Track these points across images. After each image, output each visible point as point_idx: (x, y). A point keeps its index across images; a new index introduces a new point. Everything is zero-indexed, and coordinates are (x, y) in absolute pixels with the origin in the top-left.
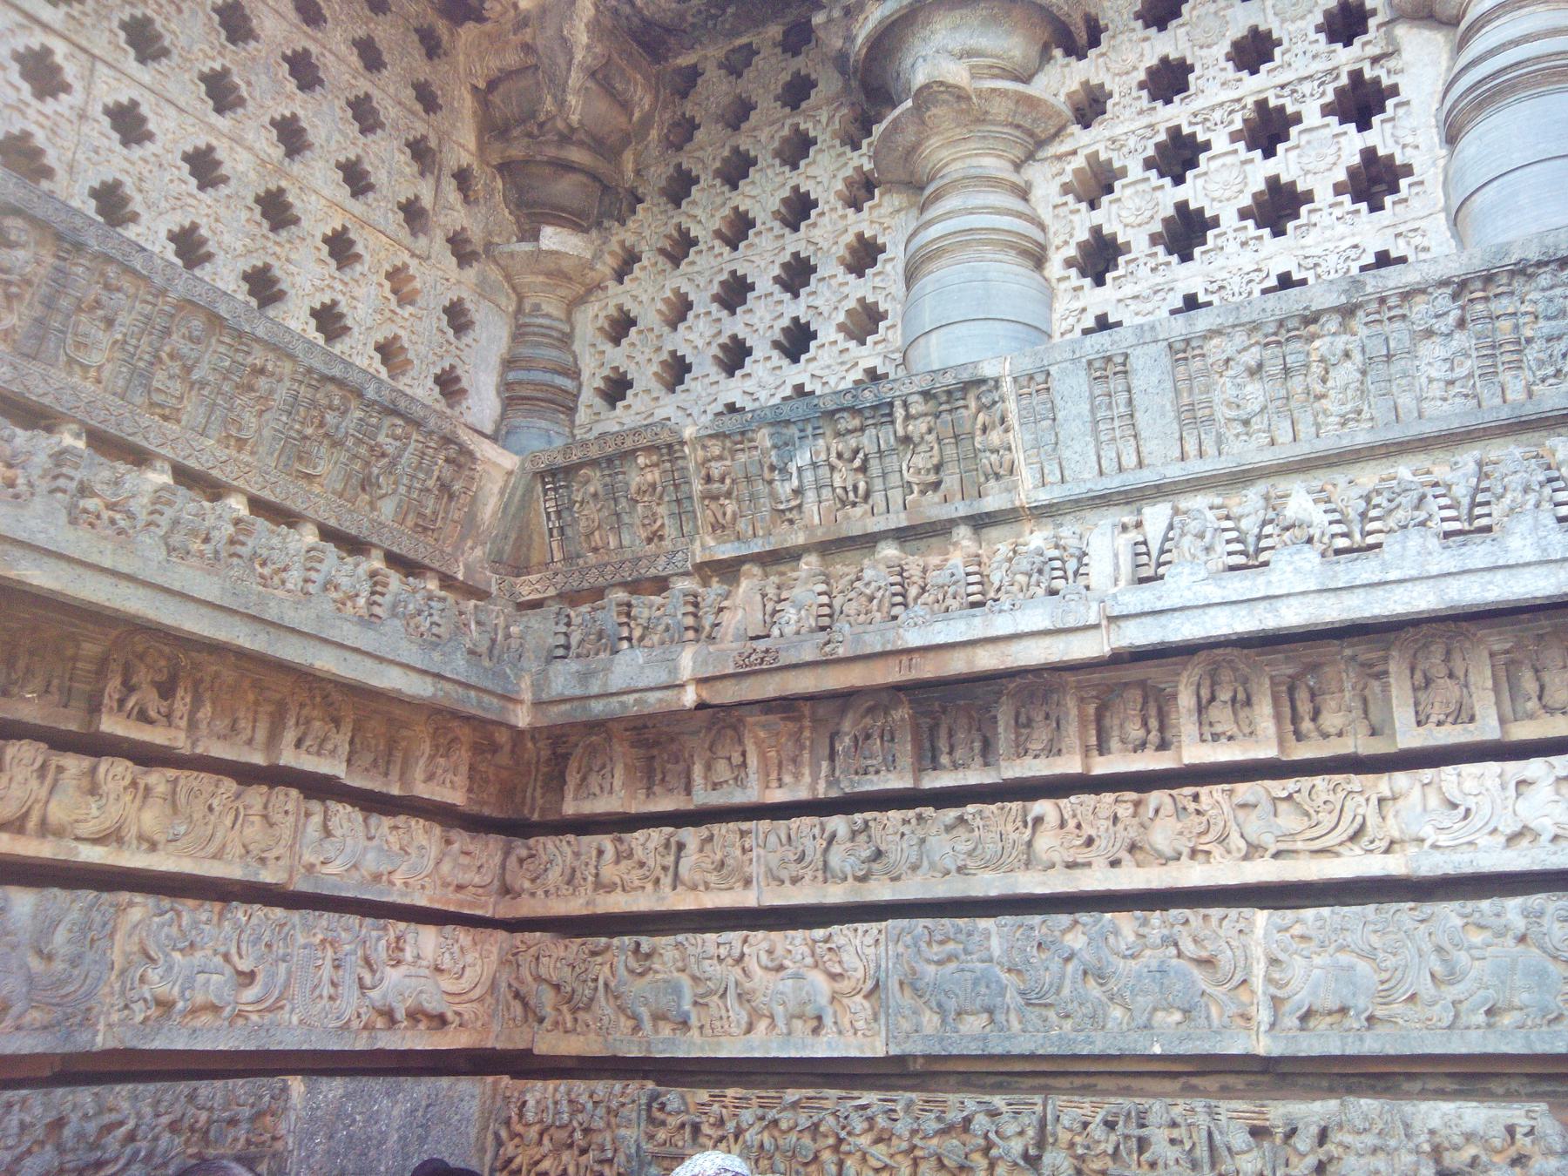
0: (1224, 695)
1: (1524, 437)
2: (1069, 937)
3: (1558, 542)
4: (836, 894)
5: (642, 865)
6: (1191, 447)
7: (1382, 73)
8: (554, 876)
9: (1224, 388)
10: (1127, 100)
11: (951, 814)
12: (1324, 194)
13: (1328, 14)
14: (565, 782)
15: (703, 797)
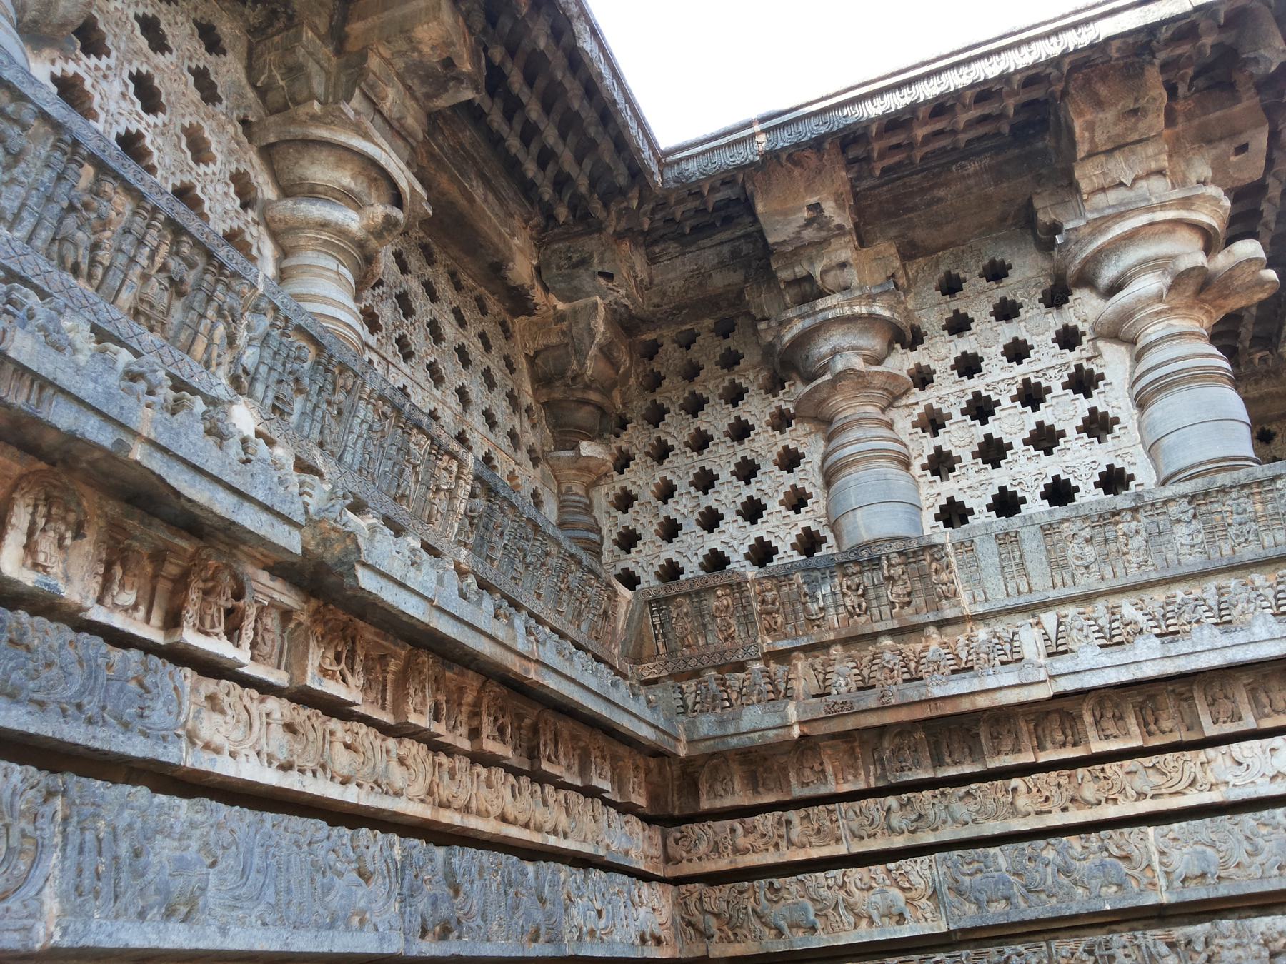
0: (1110, 715)
1: (1234, 574)
2: (1044, 853)
3: (1278, 629)
4: (899, 842)
5: (763, 836)
6: (1058, 581)
7: (1094, 367)
8: (703, 848)
9: (1074, 549)
10: (946, 375)
11: (963, 790)
12: (1071, 433)
13: (1057, 332)
14: (697, 790)
15: (798, 792)
